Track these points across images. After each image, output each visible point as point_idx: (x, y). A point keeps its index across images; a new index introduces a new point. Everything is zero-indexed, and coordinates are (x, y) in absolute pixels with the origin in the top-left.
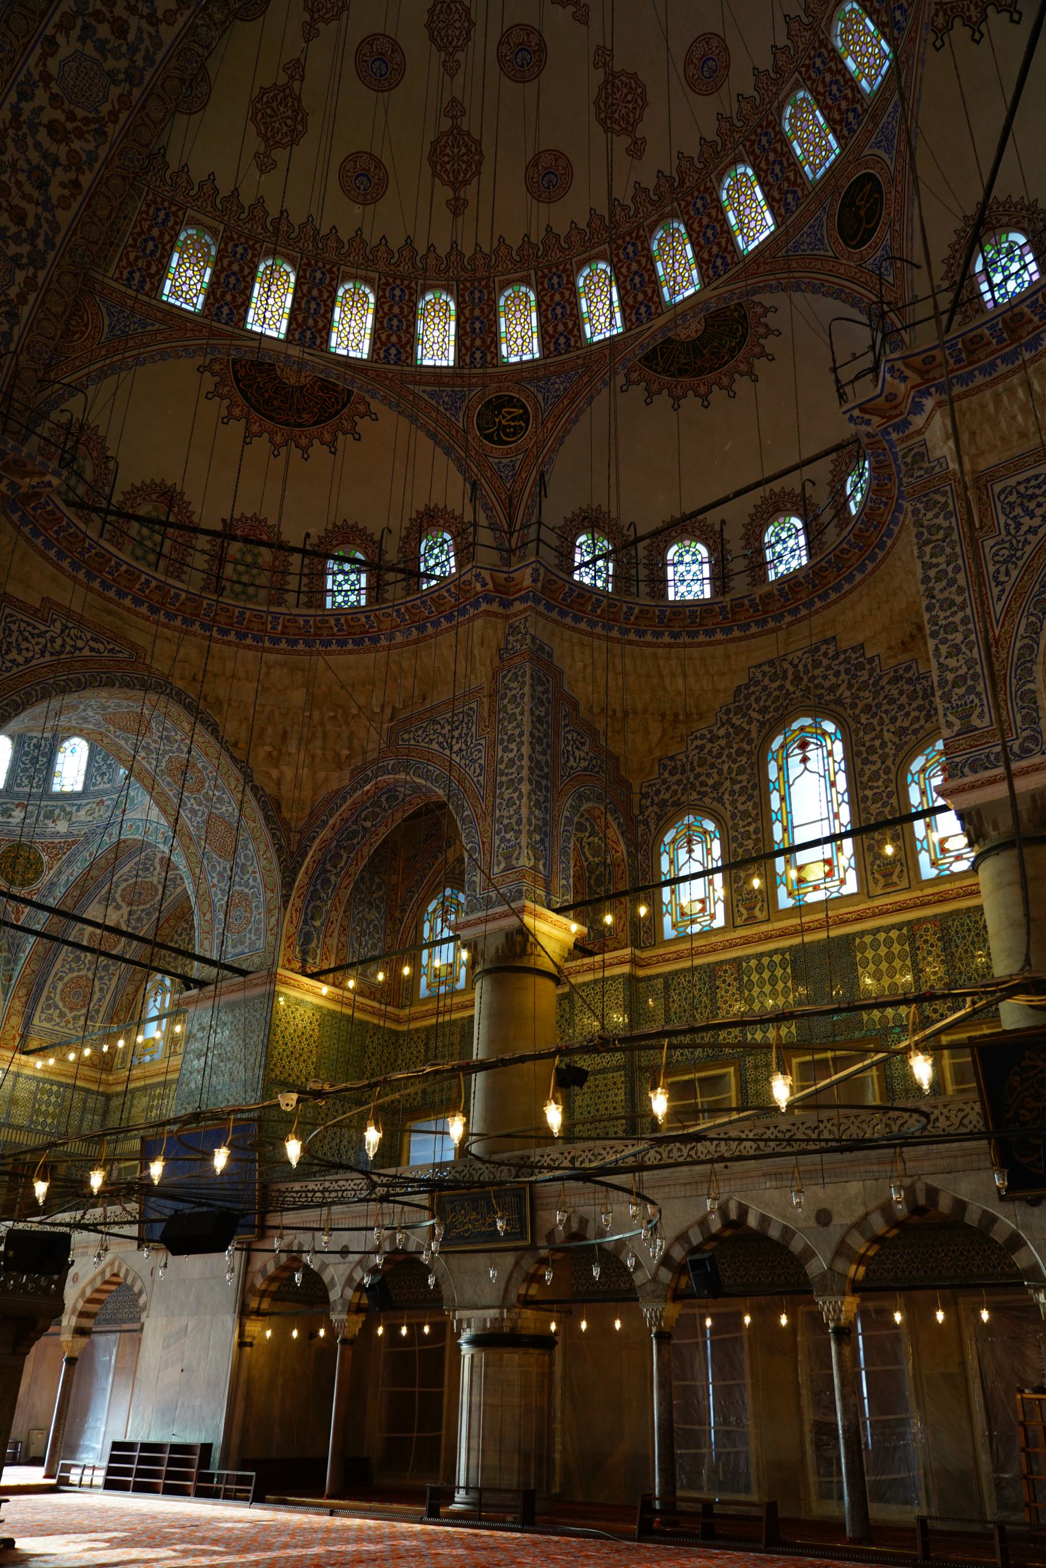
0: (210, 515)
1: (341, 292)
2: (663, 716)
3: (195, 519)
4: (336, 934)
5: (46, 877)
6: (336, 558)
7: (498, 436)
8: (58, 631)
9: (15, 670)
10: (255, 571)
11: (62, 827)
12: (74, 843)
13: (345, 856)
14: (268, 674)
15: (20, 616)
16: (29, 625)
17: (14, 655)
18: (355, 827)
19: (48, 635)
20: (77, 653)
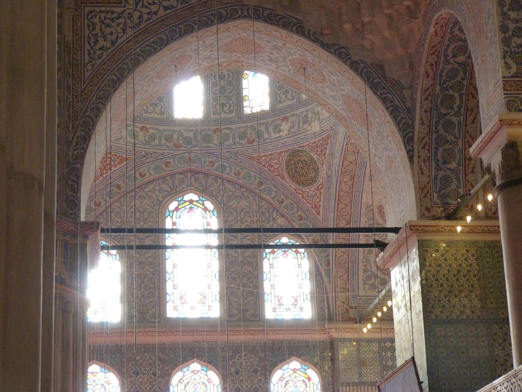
5: (323, 173)
11: (316, 127)
12: (328, 137)
13: (456, 95)
15: (98, 9)
17: (101, 43)
18: (449, 67)
20: (155, 17)
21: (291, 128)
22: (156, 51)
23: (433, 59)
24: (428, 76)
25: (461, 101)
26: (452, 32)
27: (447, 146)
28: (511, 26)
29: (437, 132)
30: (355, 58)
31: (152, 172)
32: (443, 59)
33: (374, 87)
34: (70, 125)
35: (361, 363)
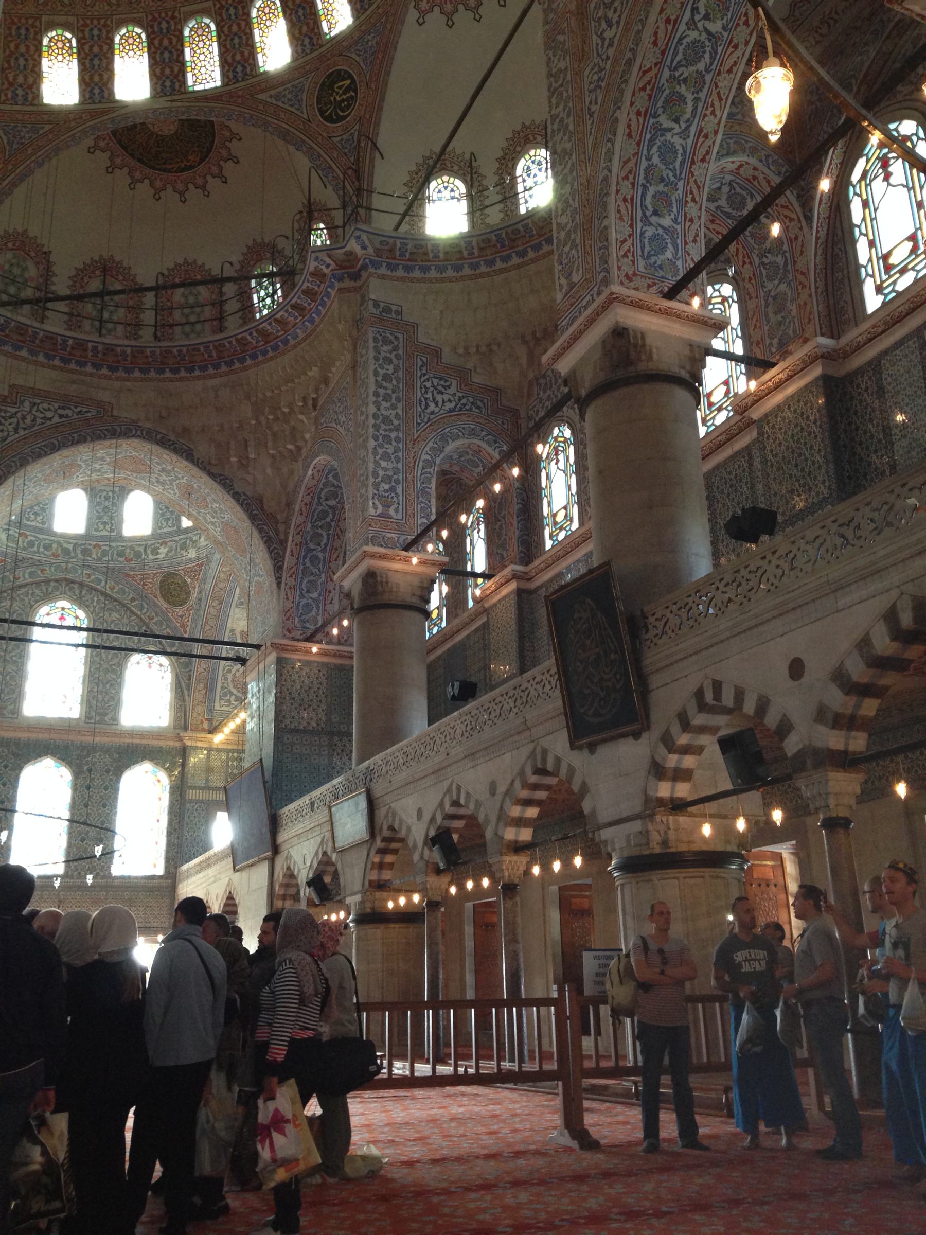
0: (146, 274)
1: (186, 32)
2: (523, 337)
3: (139, 279)
4: (336, 601)
5: (194, 595)
6: (255, 277)
7: (337, 114)
8: (28, 409)
10: (198, 310)
11: (192, 554)
12: (202, 564)
13: (324, 534)
14: (217, 396)
18: (321, 508)
19: (19, 415)
20: (48, 423)
22: (46, 454)
23: (308, 499)
26: (327, 478)
27: (312, 578)
28: (381, 473)
31: (27, 576)
33: (253, 518)
35: (209, 770)
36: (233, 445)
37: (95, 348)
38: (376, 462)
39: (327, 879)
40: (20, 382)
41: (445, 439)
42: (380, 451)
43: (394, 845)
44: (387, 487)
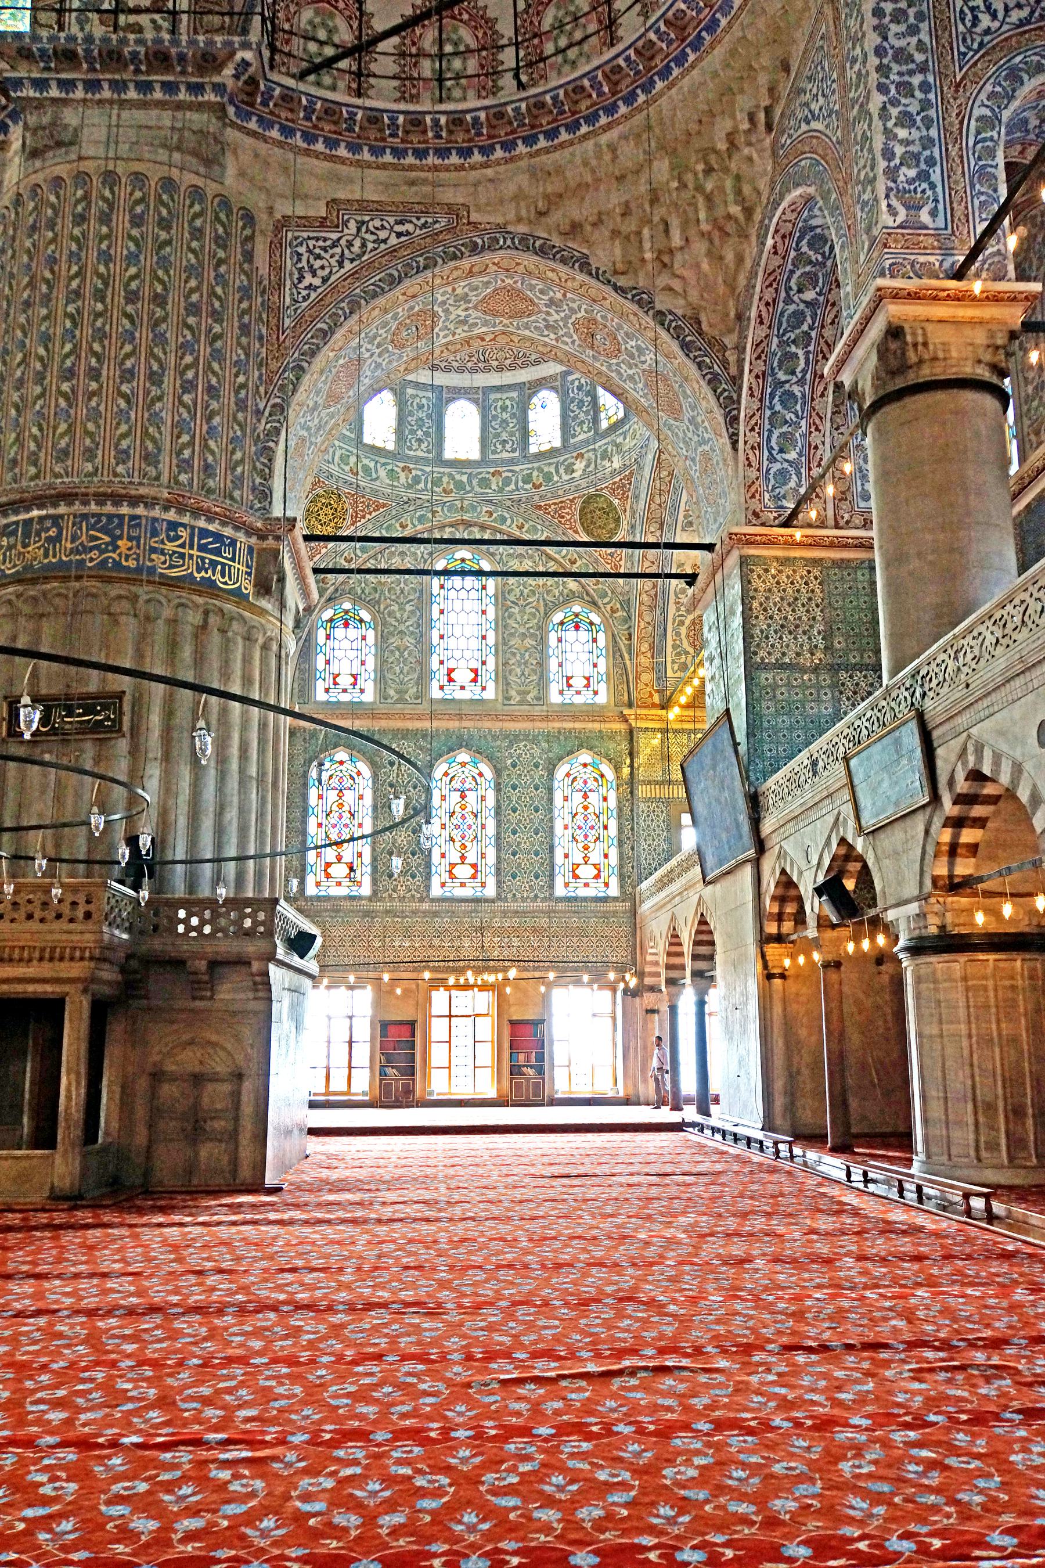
8: (354, 231)
9: (313, 295)
13: (801, 353)
15: (305, 235)
16: (317, 239)
17: (309, 279)
18: (792, 308)
19: (343, 242)
20: (383, 246)
21: (587, 466)
24: (761, 323)
25: (807, 363)
26: (797, 249)
27: (785, 429)
28: (899, 150)
29: (771, 408)
30: (658, 306)
32: (783, 294)
34: (262, 389)
36: (646, 232)
37: (436, 122)
38: (887, 131)
39: (850, 884)
40: (341, 195)
41: (1015, 77)
42: (894, 112)
43: (978, 811)
44: (912, 173)
